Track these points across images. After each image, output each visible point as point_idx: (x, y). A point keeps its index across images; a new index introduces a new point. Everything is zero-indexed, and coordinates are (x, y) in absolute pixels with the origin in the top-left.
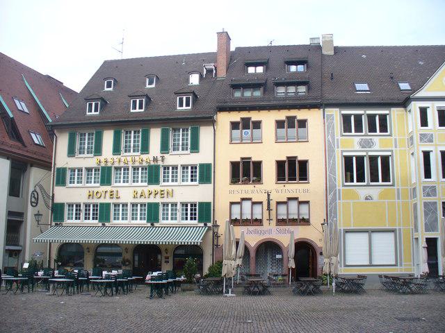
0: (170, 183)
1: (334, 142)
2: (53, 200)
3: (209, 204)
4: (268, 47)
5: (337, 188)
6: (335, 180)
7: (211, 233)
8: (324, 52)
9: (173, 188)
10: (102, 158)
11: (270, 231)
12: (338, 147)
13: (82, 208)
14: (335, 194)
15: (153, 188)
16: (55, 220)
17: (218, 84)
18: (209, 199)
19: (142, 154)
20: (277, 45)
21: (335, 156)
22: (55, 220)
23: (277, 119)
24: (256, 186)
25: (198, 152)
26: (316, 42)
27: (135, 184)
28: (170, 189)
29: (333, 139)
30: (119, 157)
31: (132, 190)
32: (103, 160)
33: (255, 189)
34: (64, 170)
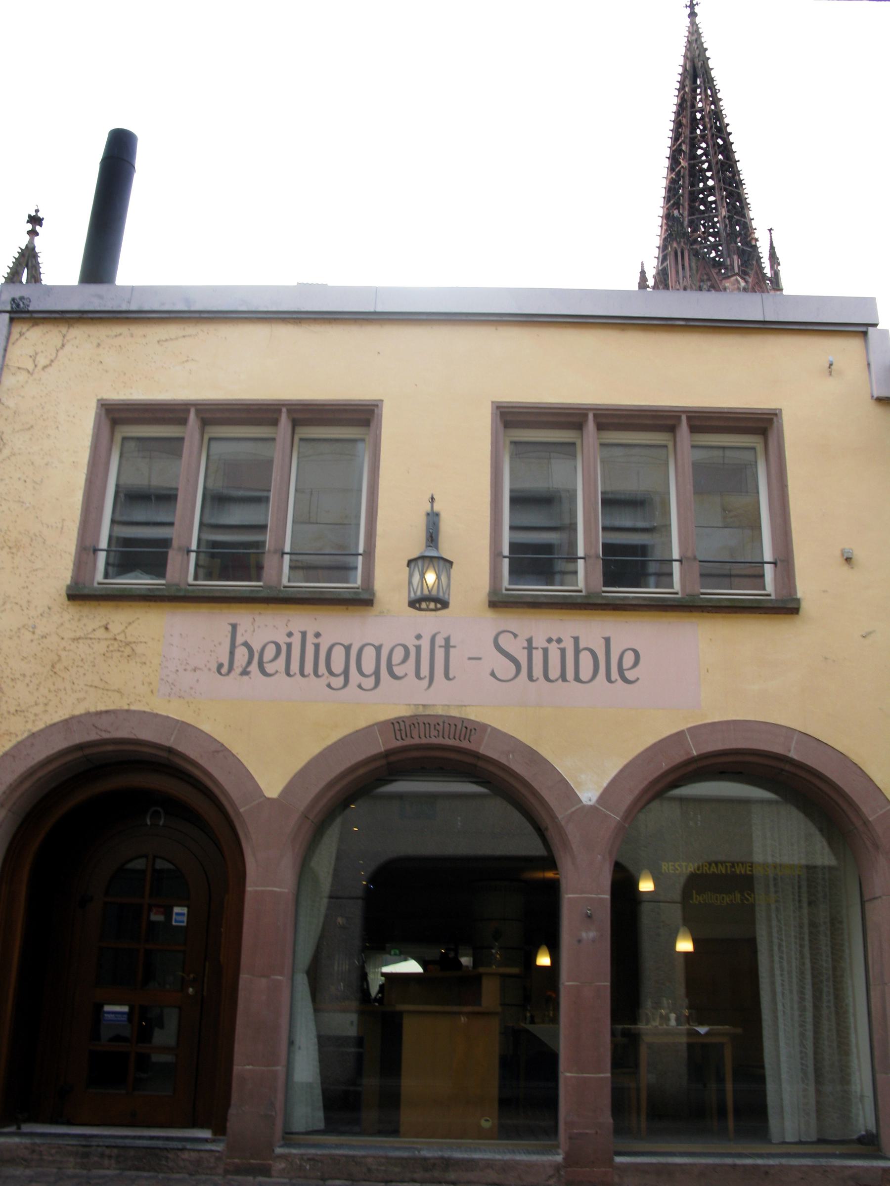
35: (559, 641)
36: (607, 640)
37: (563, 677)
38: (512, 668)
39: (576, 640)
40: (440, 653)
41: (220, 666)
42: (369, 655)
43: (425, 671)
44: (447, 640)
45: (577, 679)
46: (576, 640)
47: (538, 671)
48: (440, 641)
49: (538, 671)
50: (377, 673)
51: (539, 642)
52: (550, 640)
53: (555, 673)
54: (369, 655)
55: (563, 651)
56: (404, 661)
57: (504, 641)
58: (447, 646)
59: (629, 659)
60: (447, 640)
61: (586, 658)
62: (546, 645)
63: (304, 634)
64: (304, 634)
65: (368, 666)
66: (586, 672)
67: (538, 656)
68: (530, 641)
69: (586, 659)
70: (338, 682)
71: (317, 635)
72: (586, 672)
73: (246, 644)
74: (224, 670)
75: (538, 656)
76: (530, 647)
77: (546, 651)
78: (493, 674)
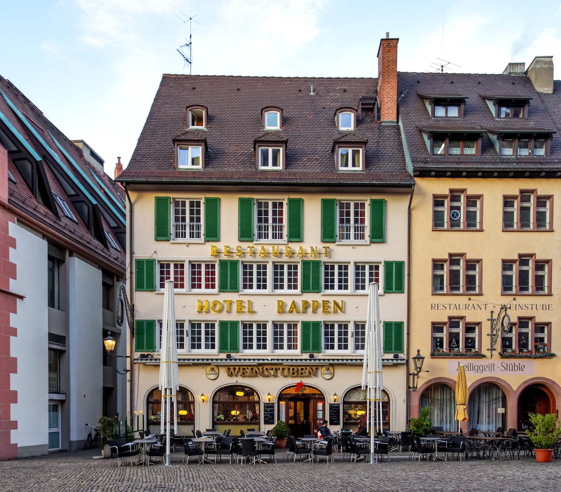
0: (336, 291)
2: (133, 315)
3: (399, 325)
9: (344, 298)
10: (221, 246)
11: (492, 367)
13: (185, 330)
15: (310, 297)
16: (139, 347)
17: (387, 132)
18: (401, 317)
19: (289, 241)
20: (450, 72)
22: (139, 347)
25: (383, 242)
27: (279, 291)
28: (339, 300)
30: (251, 244)
31: (274, 301)
32: (223, 250)
33: (471, 303)
34: (151, 262)
36: (519, 364)
39: (514, 364)
40: (493, 367)
41: (457, 369)
42: (481, 367)
43: (490, 369)
46: (514, 364)
48: (492, 364)
53: (511, 369)
54: (481, 367)
55: (512, 366)
58: (494, 365)
59: (523, 367)
61: (516, 367)
63: (470, 364)
64: (470, 364)
65: (481, 369)
66: (516, 369)
67: (508, 366)
68: (507, 364)
69: (516, 367)
72: (516, 369)
75: (508, 366)
76: (507, 365)
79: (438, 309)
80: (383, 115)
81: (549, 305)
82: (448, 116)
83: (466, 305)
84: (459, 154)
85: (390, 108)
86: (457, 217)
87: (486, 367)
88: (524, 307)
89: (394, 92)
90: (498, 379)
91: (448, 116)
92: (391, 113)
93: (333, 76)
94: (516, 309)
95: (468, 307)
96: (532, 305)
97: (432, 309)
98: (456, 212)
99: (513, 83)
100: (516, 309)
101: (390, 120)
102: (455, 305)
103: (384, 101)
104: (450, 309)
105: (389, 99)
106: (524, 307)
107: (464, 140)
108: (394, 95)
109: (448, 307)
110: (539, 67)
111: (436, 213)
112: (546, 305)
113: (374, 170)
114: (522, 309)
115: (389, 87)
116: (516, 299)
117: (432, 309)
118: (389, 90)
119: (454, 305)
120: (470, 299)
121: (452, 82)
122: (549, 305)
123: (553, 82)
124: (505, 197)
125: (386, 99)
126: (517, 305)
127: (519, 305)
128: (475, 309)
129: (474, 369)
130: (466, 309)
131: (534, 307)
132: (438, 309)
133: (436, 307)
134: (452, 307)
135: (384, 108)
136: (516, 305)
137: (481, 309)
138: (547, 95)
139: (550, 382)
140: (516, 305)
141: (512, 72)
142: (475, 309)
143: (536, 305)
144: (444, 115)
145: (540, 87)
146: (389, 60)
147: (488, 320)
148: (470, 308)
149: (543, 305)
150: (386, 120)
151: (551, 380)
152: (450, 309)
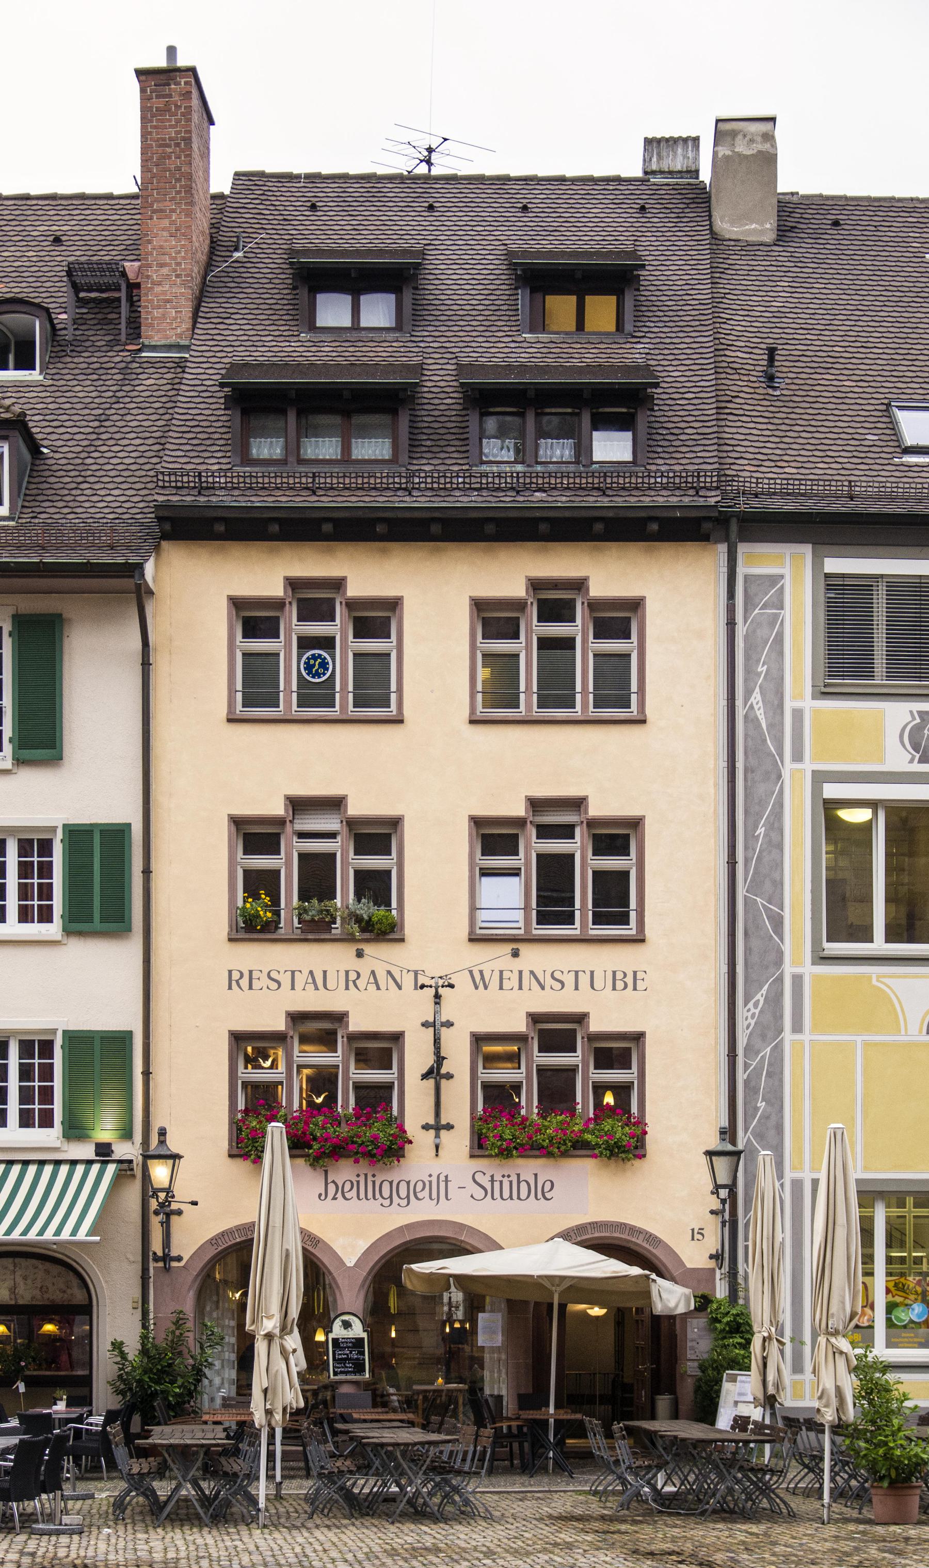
1: (776, 727)
4: (411, 178)
5: (789, 970)
6: (778, 923)
7: (132, 1194)
8: (725, 226)
12: (798, 757)
14: (775, 999)
21: (780, 804)
23: (472, 595)
24: (368, 949)
26: (678, 163)
29: (776, 706)
33: (365, 966)
35: (509, 1176)
36: (536, 1175)
37: (511, 1197)
38: (483, 1192)
39: (518, 1175)
40: (442, 1185)
41: (320, 1195)
43: (434, 1195)
44: (446, 1177)
45: (519, 1198)
46: (518, 1175)
47: (497, 1194)
48: (442, 1178)
49: (497, 1194)
50: (408, 1197)
51: (498, 1177)
52: (503, 1176)
53: (506, 1194)
54: (403, 1186)
55: (511, 1182)
56: (423, 1189)
57: (479, 1177)
58: (447, 1181)
59: (548, 1186)
60: (446, 1177)
61: (524, 1186)
62: (501, 1179)
65: (403, 1193)
66: (524, 1194)
67: (497, 1185)
68: (492, 1176)
69: (524, 1186)
70: (387, 1202)
71: (374, 1176)
72: (524, 1194)
73: (333, 1182)
74: (323, 1197)
75: (497, 1185)
76: (492, 1181)
77: (501, 1182)
78: (472, 1196)
79: (251, 988)
80: (147, 325)
81: (635, 973)
82: (363, 324)
83: (347, 972)
84: (387, 458)
85: (168, 301)
86: (324, 674)
87: (420, 1186)
88: (549, 982)
89: (183, 246)
90: (462, 1227)
91: (363, 324)
92: (175, 318)
93: (35, 190)
94: (520, 988)
95: (354, 982)
96: (577, 972)
97: (230, 988)
98: (320, 655)
99: (643, 208)
100: (520, 988)
101: (168, 342)
102: (311, 972)
103: (148, 277)
104: (293, 988)
105: (165, 271)
106: (549, 982)
107: (347, 414)
108: (184, 258)
109: (286, 980)
110: (728, 153)
111: (252, 658)
112: (625, 975)
113: (50, 512)
114: (543, 988)
115: (163, 229)
116: (520, 953)
117: (230, 988)
118: (166, 241)
119: (306, 973)
120: (360, 954)
121: (431, 208)
122: (635, 973)
123: (774, 201)
124: (479, 606)
125: (157, 271)
126: (526, 975)
127: (532, 972)
128: (378, 988)
129: (378, 1195)
130: (347, 988)
131: (584, 980)
132: (251, 988)
133: (245, 982)
134: (300, 979)
135: (148, 301)
136: (521, 972)
137: (400, 988)
138: (749, 248)
139: (641, 1237)
140: (521, 972)
141: (654, 167)
142: (378, 988)
143: (592, 973)
144: (347, 322)
145: (732, 223)
146: (164, 139)
147: (425, 1025)
148: (361, 983)
149: (614, 973)
150: (157, 340)
151: (647, 1232)
152: (293, 988)
